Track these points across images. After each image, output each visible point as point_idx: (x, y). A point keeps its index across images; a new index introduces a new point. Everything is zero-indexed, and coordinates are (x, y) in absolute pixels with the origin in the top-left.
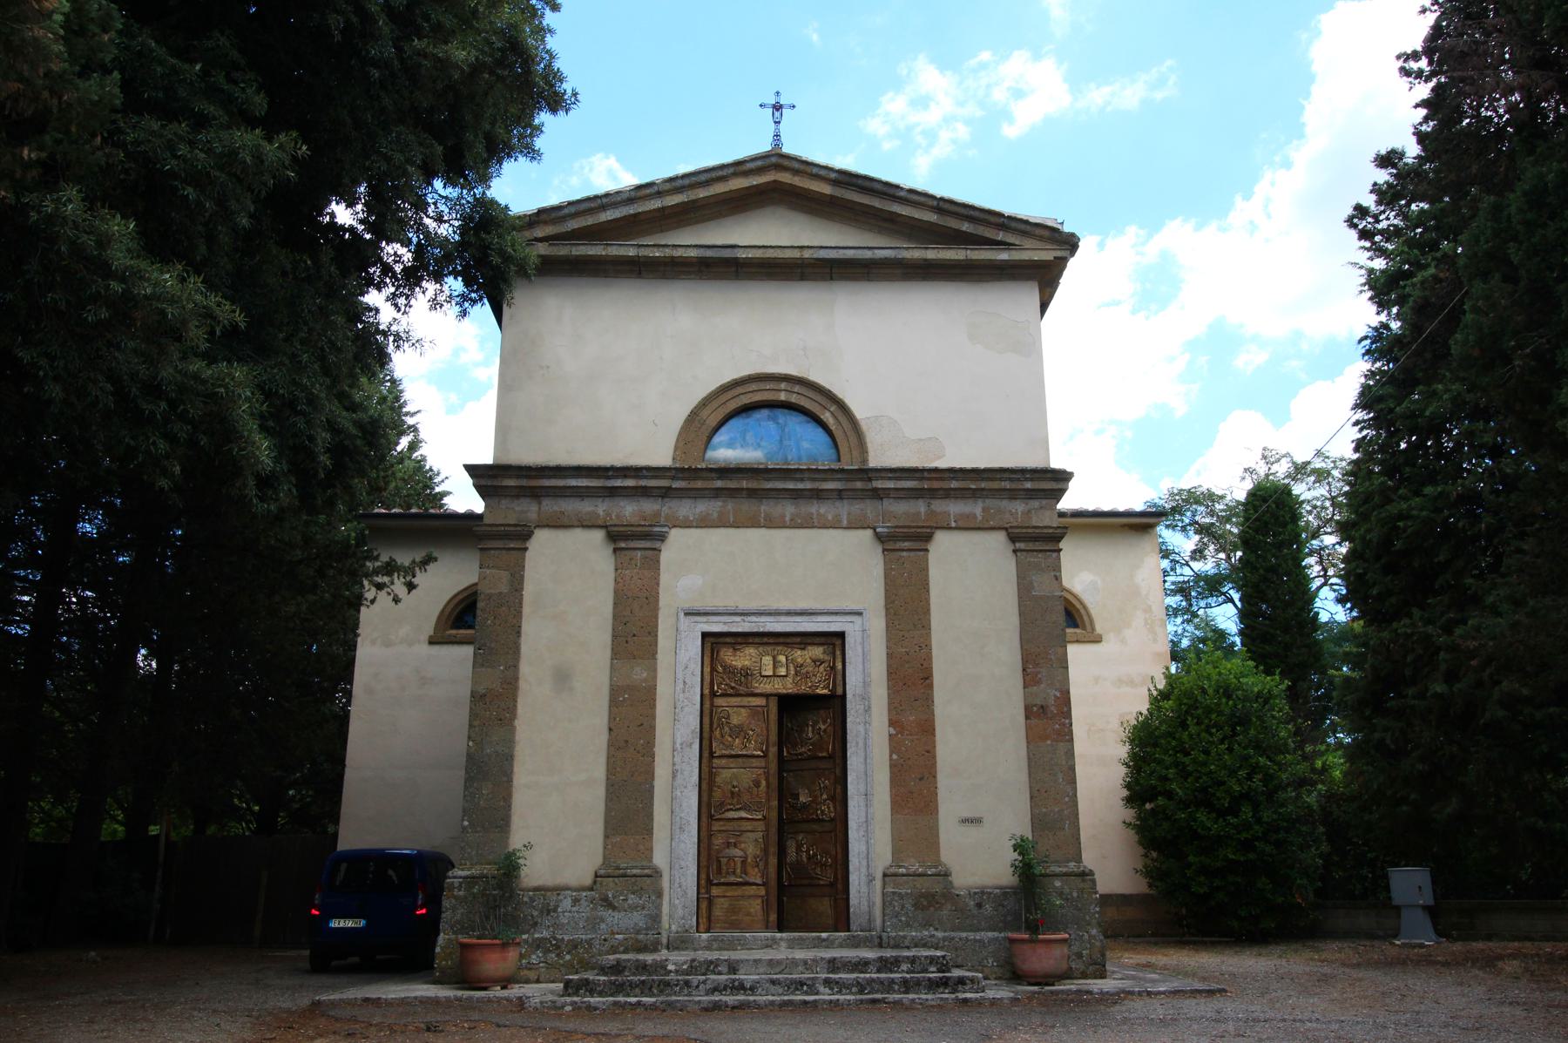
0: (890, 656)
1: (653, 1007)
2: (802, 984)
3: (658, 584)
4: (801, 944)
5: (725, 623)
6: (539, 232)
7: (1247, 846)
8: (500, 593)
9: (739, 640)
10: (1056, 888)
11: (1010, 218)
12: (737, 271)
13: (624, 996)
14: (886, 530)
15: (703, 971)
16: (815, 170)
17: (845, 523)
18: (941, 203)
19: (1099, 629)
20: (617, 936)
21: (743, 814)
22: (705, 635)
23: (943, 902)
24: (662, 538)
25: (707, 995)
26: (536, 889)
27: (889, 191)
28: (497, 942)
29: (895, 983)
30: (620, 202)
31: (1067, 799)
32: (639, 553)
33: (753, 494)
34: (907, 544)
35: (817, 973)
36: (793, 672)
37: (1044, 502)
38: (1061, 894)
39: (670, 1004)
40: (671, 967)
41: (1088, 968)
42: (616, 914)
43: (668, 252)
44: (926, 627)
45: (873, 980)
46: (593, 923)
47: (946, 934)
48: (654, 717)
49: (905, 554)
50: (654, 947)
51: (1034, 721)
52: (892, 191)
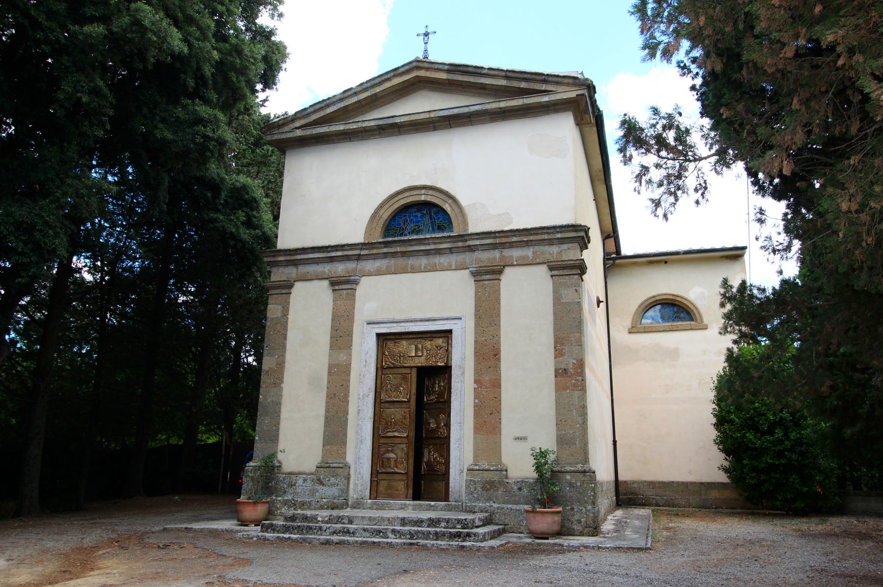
0: (476, 342)
1: (296, 540)
2: (380, 532)
3: (354, 308)
4: (430, 508)
5: (388, 328)
6: (297, 124)
7: (780, 454)
8: (277, 317)
9: (397, 337)
10: (567, 480)
11: (548, 75)
12: (399, 131)
13: (289, 534)
14: (474, 269)
15: (336, 521)
16: (436, 66)
17: (454, 267)
18: (507, 73)
19: (705, 321)
20: (324, 500)
21: (396, 434)
22: (379, 335)
23: (499, 486)
24: (356, 283)
25: (330, 535)
26: (291, 473)
27: (477, 71)
28: (251, 501)
29: (431, 534)
30: (336, 101)
31: (578, 426)
32: (345, 292)
33: (404, 254)
34: (488, 277)
35: (395, 526)
36: (425, 354)
37: (570, 245)
38: (571, 485)
39: (304, 540)
40: (319, 519)
41: (584, 530)
42: (324, 488)
43: (360, 125)
44: (498, 325)
45: (418, 532)
46: (313, 492)
47: (500, 506)
48: (349, 381)
49: (486, 282)
50: (345, 505)
51: (559, 378)
52: (478, 71)
